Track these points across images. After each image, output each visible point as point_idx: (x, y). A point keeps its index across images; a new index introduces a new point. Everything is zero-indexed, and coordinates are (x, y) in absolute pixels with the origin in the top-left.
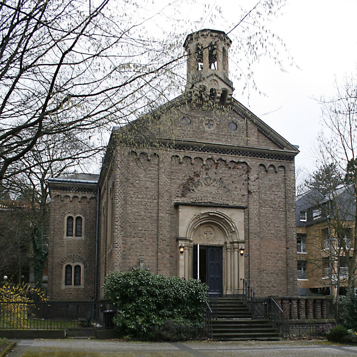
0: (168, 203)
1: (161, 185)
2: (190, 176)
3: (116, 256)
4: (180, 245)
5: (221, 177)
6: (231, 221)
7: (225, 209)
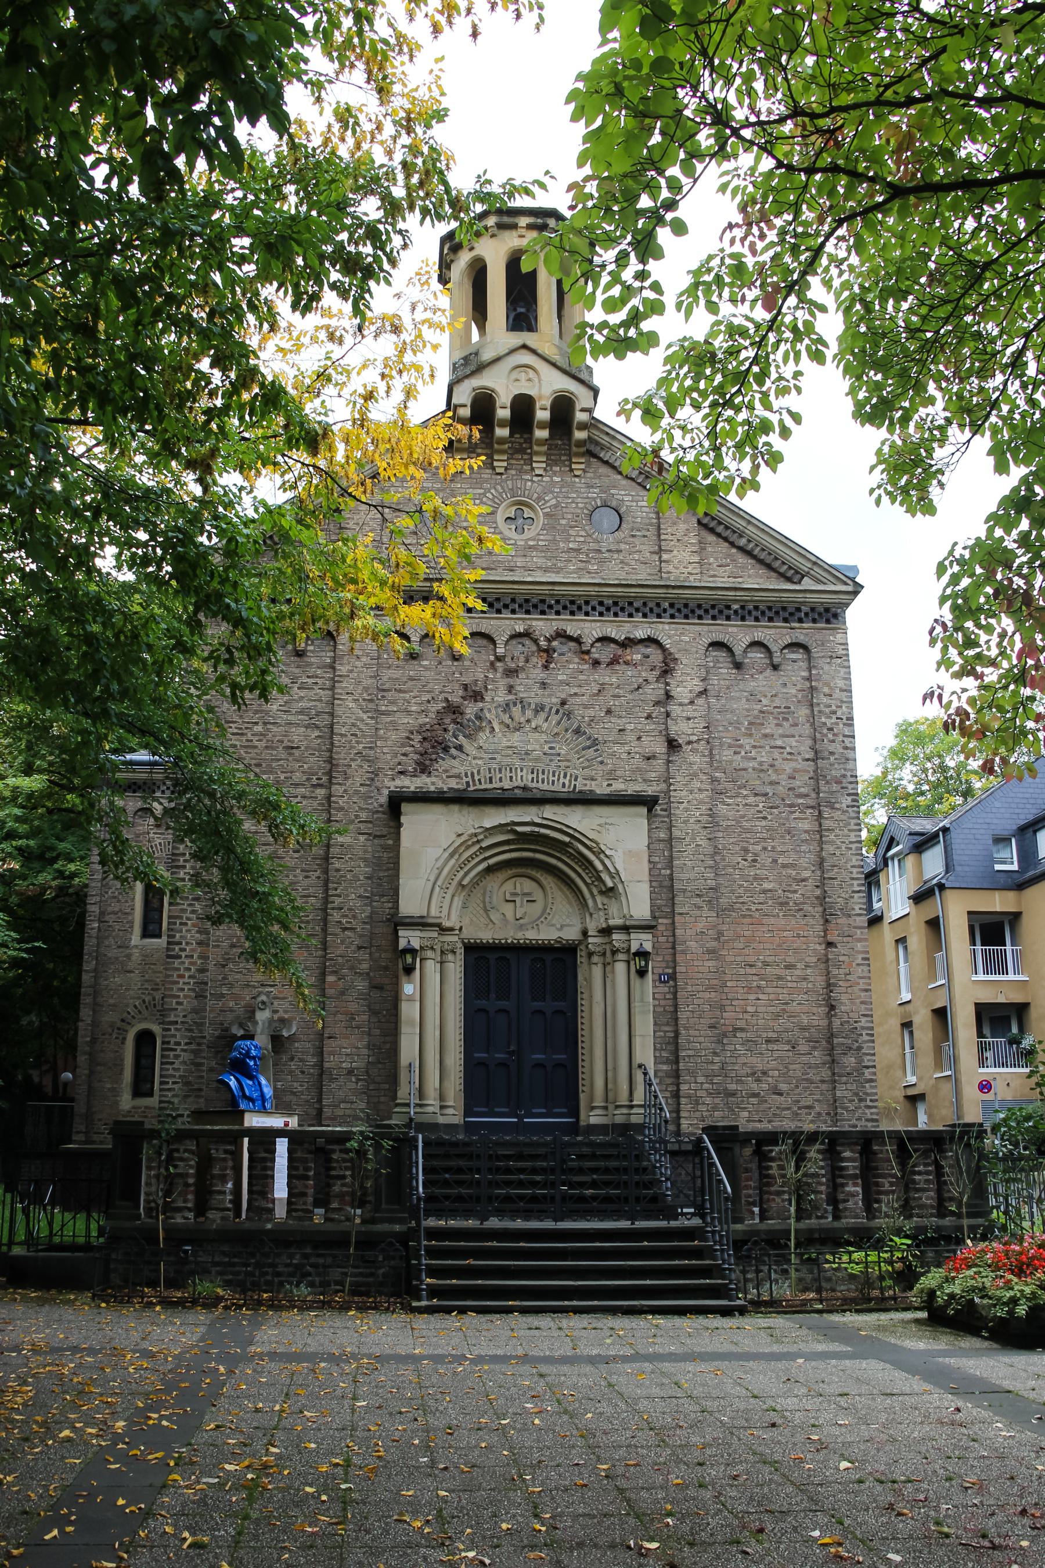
0: (367, 797)
1: (342, 735)
2: (447, 700)
3: (175, 987)
4: (402, 944)
5: (563, 696)
6: (599, 852)
7: (574, 808)
